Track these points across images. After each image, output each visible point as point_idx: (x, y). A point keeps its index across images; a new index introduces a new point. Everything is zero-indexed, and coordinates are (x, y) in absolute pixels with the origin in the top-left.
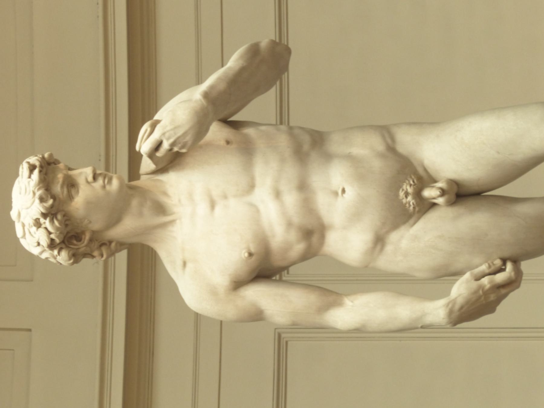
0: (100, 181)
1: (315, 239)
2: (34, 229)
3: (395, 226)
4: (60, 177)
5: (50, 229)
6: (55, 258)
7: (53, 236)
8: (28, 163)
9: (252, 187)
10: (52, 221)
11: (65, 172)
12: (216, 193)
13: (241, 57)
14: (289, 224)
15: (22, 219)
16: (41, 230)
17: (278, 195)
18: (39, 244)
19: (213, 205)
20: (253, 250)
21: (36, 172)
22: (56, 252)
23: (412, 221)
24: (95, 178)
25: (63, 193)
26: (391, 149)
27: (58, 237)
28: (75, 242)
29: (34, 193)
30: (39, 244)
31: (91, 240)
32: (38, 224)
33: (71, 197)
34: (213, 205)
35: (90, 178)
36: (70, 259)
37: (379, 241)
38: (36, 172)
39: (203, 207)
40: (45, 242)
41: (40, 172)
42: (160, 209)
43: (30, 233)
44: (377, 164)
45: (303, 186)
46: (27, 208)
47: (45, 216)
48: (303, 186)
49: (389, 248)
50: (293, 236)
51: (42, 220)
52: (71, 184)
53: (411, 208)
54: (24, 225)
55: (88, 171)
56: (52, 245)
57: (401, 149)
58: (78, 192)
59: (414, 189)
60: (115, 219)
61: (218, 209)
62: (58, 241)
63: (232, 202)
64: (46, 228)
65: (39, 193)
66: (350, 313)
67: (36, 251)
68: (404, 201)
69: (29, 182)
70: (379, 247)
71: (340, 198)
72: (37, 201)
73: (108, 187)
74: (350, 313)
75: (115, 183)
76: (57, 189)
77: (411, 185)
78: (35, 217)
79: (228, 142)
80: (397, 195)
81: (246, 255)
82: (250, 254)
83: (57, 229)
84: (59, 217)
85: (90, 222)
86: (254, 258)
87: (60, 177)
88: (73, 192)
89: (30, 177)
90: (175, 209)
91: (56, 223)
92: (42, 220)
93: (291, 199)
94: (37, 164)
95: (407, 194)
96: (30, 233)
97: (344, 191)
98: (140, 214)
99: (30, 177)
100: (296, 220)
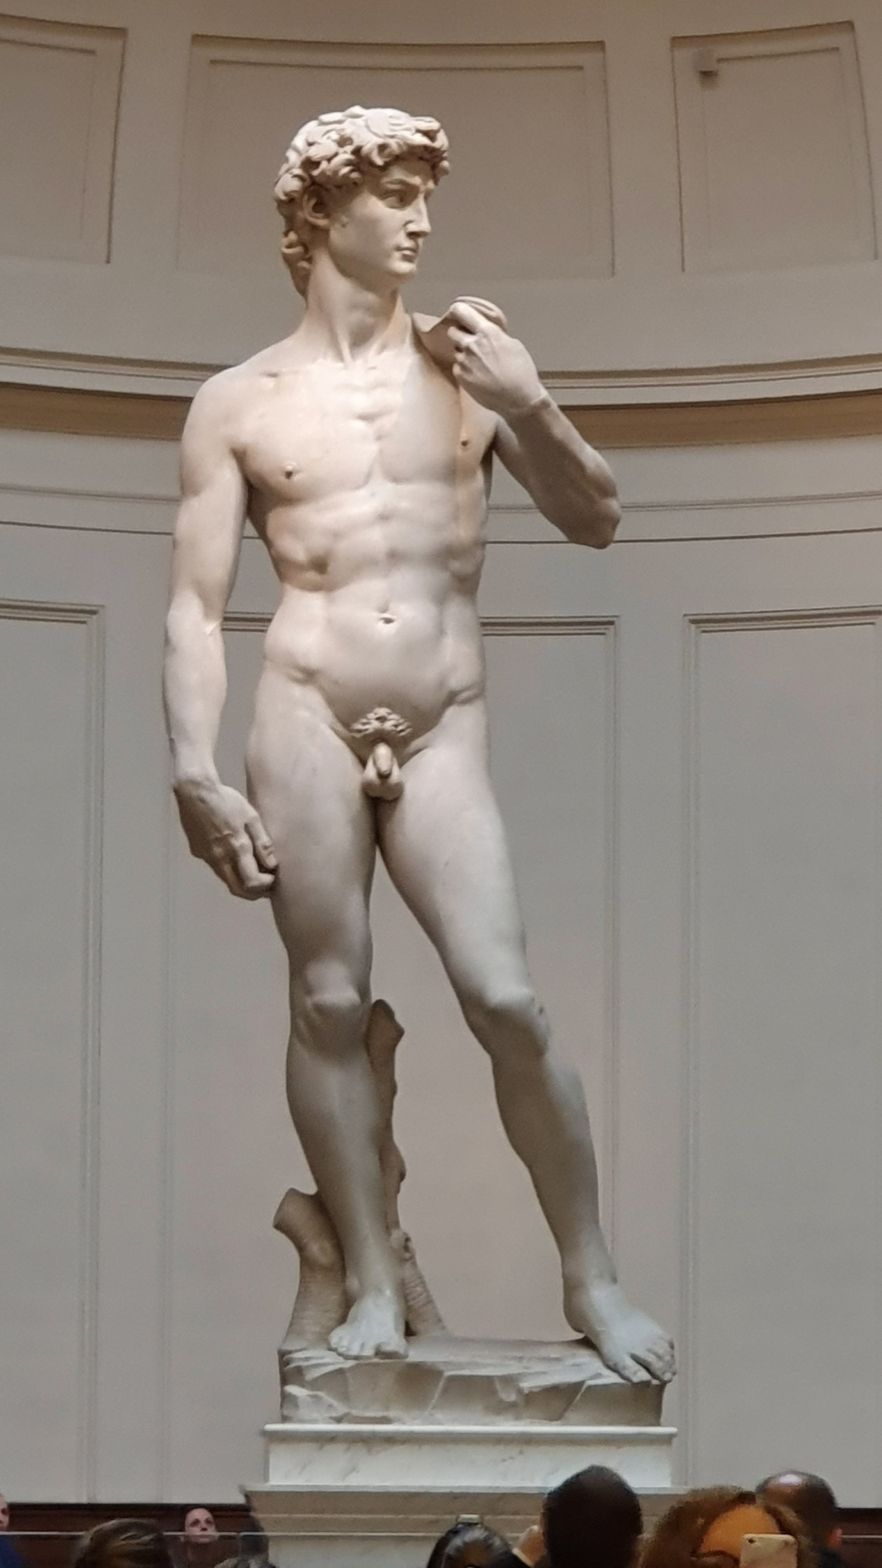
0: (407, 243)
1: (312, 576)
2: (335, 136)
3: (331, 702)
4: (416, 180)
5: (336, 161)
6: (287, 171)
7: (324, 165)
8: (438, 131)
9: (396, 479)
10: (348, 163)
11: (422, 188)
12: (386, 422)
13: (598, 466)
14: (337, 535)
15: (350, 119)
16: (334, 148)
17: (384, 517)
18: (310, 144)
19: (367, 418)
20: (296, 478)
21: (425, 141)
22: (298, 171)
23: (340, 727)
24: (413, 235)
25: (392, 183)
26: (451, 699)
27: (323, 173)
28: (313, 202)
29: (392, 137)
30: (310, 144)
31: (314, 228)
32: (343, 141)
33: (384, 195)
34: (367, 418)
35: (412, 228)
36: (286, 194)
37: (309, 676)
38: (425, 141)
39: (362, 402)
40: (315, 153)
41: (425, 147)
42: (361, 338)
43: (328, 132)
44: (429, 674)
45: (395, 558)
46: (367, 127)
47: (357, 151)
48: (395, 558)
49: (297, 691)
50: (318, 543)
51: (349, 148)
52: (404, 196)
53: (360, 727)
54: (340, 122)
55: (424, 225)
56: (309, 164)
57: (451, 712)
58: (392, 207)
59: (389, 732)
60: (346, 266)
61: (361, 425)
62: (316, 173)
63: (372, 448)
64: (336, 154)
65: (393, 143)
66: (196, 630)
67: (299, 141)
68: (371, 716)
69: (408, 129)
70: (299, 675)
71: (376, 615)
72: (381, 141)
73: (397, 254)
74: (196, 630)
75: (404, 267)
76: (397, 174)
77: (396, 726)
78: (354, 137)
79: (464, 444)
80: (380, 705)
81: (289, 468)
82: (289, 474)
83: (336, 172)
84: (355, 175)
85: (344, 226)
86: (283, 479)
87: (416, 180)
88: (392, 199)
89: (418, 131)
90: (359, 362)
91: (346, 170)
92: (349, 148)
93: (376, 539)
94: (437, 145)
95: (382, 719)
96: (328, 132)
97: (388, 621)
98: (354, 306)
99: (418, 131)
100: (343, 548)
